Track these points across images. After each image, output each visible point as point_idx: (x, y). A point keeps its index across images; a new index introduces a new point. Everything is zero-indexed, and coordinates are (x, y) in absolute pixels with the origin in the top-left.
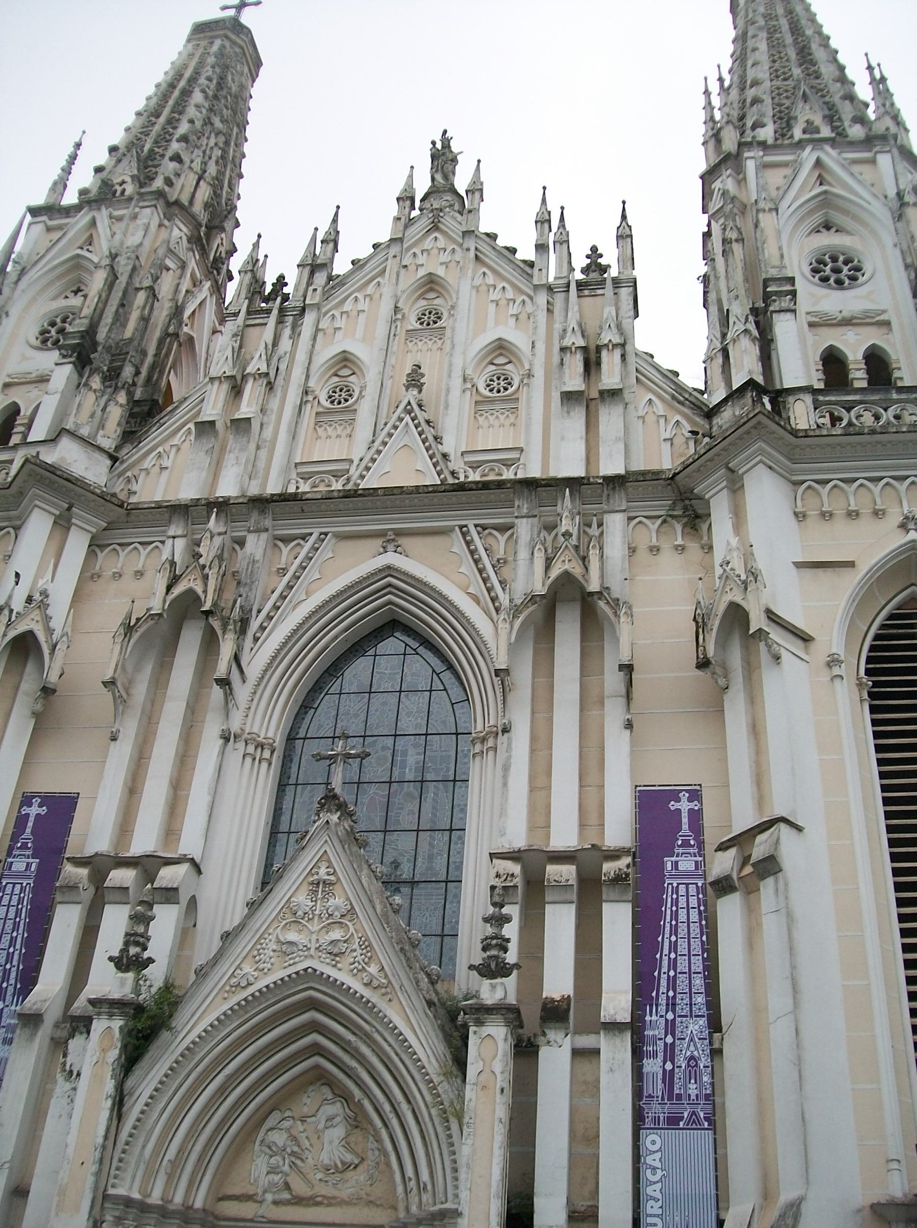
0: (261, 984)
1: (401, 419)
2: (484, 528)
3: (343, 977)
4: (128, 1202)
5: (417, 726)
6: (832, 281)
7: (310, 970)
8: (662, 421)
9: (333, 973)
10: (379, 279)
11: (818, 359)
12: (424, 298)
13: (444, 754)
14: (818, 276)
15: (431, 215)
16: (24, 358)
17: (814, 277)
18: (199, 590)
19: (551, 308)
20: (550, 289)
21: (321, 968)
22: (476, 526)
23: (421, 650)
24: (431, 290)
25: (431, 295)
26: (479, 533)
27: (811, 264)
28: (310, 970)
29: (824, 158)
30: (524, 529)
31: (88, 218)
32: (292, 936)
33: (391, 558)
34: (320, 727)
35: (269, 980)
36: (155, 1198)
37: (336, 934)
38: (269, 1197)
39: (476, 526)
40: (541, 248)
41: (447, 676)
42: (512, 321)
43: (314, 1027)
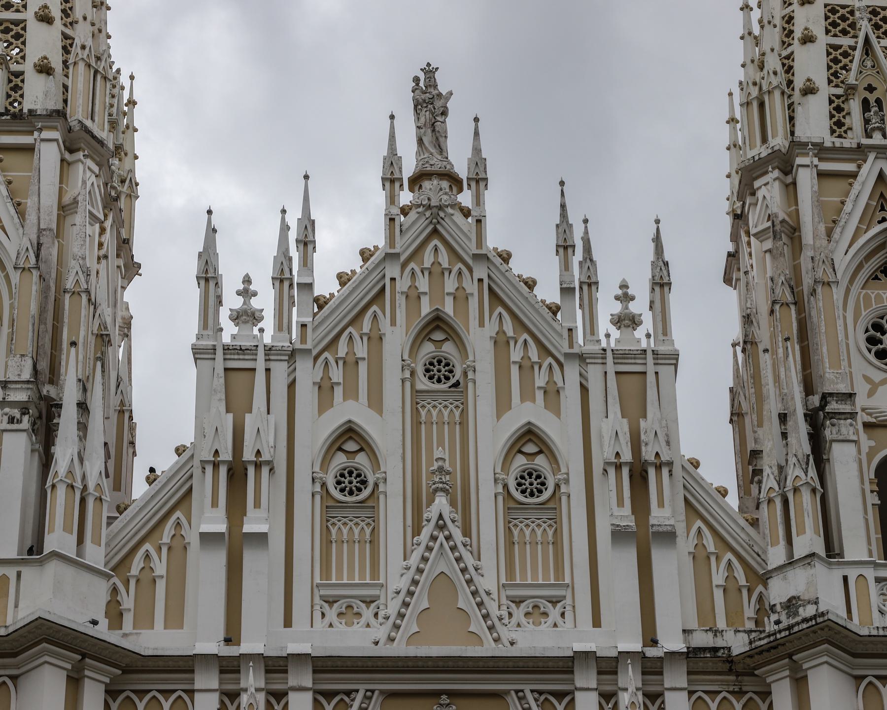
1: (434, 538)
2: (541, 693)
8: (713, 559)
10: (374, 308)
11: (872, 476)
12: (430, 340)
14: (874, 349)
15: (428, 214)
17: (870, 351)
19: (584, 382)
20: (582, 358)
22: (532, 691)
24: (438, 328)
25: (438, 336)
26: (536, 700)
27: (867, 331)
39: (532, 691)
40: (566, 291)
42: (539, 395)
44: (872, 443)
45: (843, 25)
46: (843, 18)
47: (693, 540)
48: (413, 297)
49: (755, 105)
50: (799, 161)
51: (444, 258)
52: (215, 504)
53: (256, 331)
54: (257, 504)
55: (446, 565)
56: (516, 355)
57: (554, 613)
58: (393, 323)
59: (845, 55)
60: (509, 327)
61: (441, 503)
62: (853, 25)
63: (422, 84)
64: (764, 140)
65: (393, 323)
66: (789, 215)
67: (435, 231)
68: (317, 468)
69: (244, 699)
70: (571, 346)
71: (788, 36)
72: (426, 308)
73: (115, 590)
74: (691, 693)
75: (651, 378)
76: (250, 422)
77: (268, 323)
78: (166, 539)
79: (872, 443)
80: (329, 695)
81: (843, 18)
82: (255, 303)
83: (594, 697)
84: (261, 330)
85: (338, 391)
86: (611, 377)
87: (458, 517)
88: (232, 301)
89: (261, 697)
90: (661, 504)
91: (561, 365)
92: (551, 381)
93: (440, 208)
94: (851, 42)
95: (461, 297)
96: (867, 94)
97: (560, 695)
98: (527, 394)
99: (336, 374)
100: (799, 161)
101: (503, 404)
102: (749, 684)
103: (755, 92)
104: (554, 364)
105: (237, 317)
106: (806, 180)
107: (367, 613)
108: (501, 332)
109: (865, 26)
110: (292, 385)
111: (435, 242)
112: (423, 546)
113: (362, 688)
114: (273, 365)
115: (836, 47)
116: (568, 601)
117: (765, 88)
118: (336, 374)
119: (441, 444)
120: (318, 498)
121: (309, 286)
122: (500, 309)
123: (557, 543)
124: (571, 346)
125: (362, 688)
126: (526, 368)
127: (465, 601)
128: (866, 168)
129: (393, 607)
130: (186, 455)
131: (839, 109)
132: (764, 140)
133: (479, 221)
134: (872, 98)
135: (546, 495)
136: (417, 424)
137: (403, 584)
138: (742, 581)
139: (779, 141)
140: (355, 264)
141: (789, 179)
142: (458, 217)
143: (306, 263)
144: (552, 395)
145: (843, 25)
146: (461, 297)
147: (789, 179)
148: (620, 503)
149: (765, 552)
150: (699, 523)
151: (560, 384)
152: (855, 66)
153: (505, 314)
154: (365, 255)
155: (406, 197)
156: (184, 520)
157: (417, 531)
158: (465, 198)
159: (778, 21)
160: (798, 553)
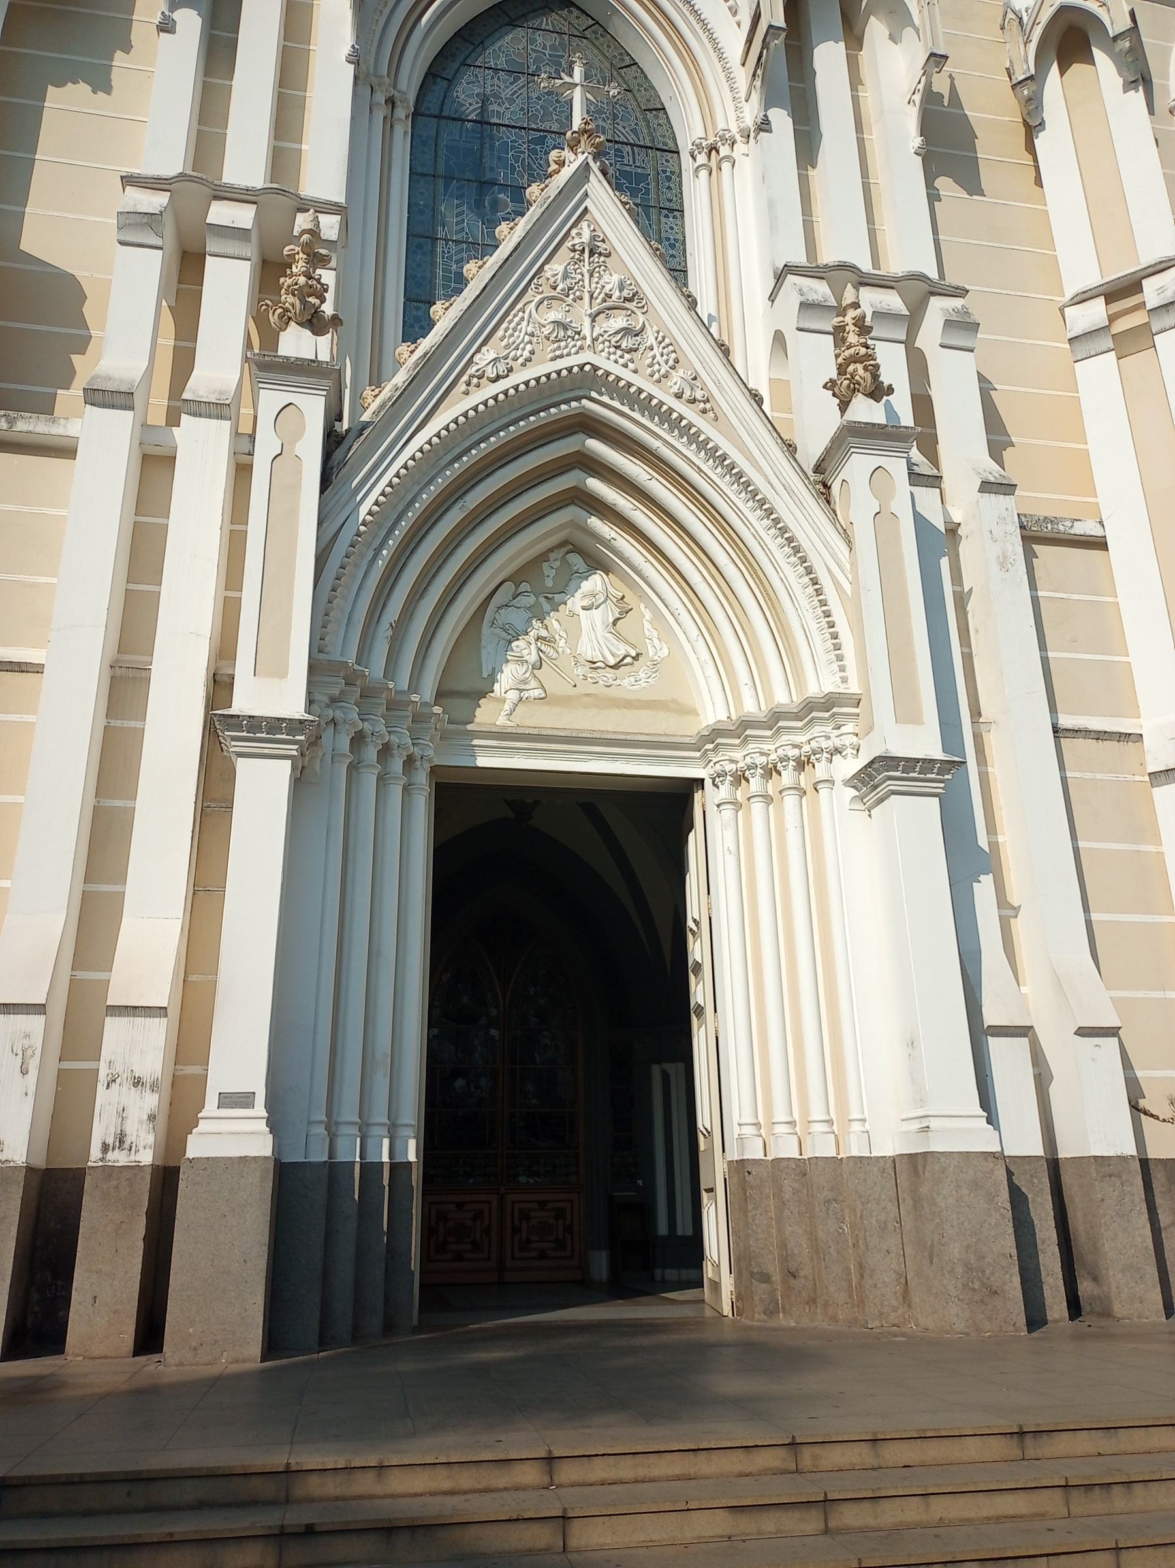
3: (638, 381)
7: (587, 368)
9: (627, 375)
13: (639, 170)
21: (606, 363)
28: (587, 368)
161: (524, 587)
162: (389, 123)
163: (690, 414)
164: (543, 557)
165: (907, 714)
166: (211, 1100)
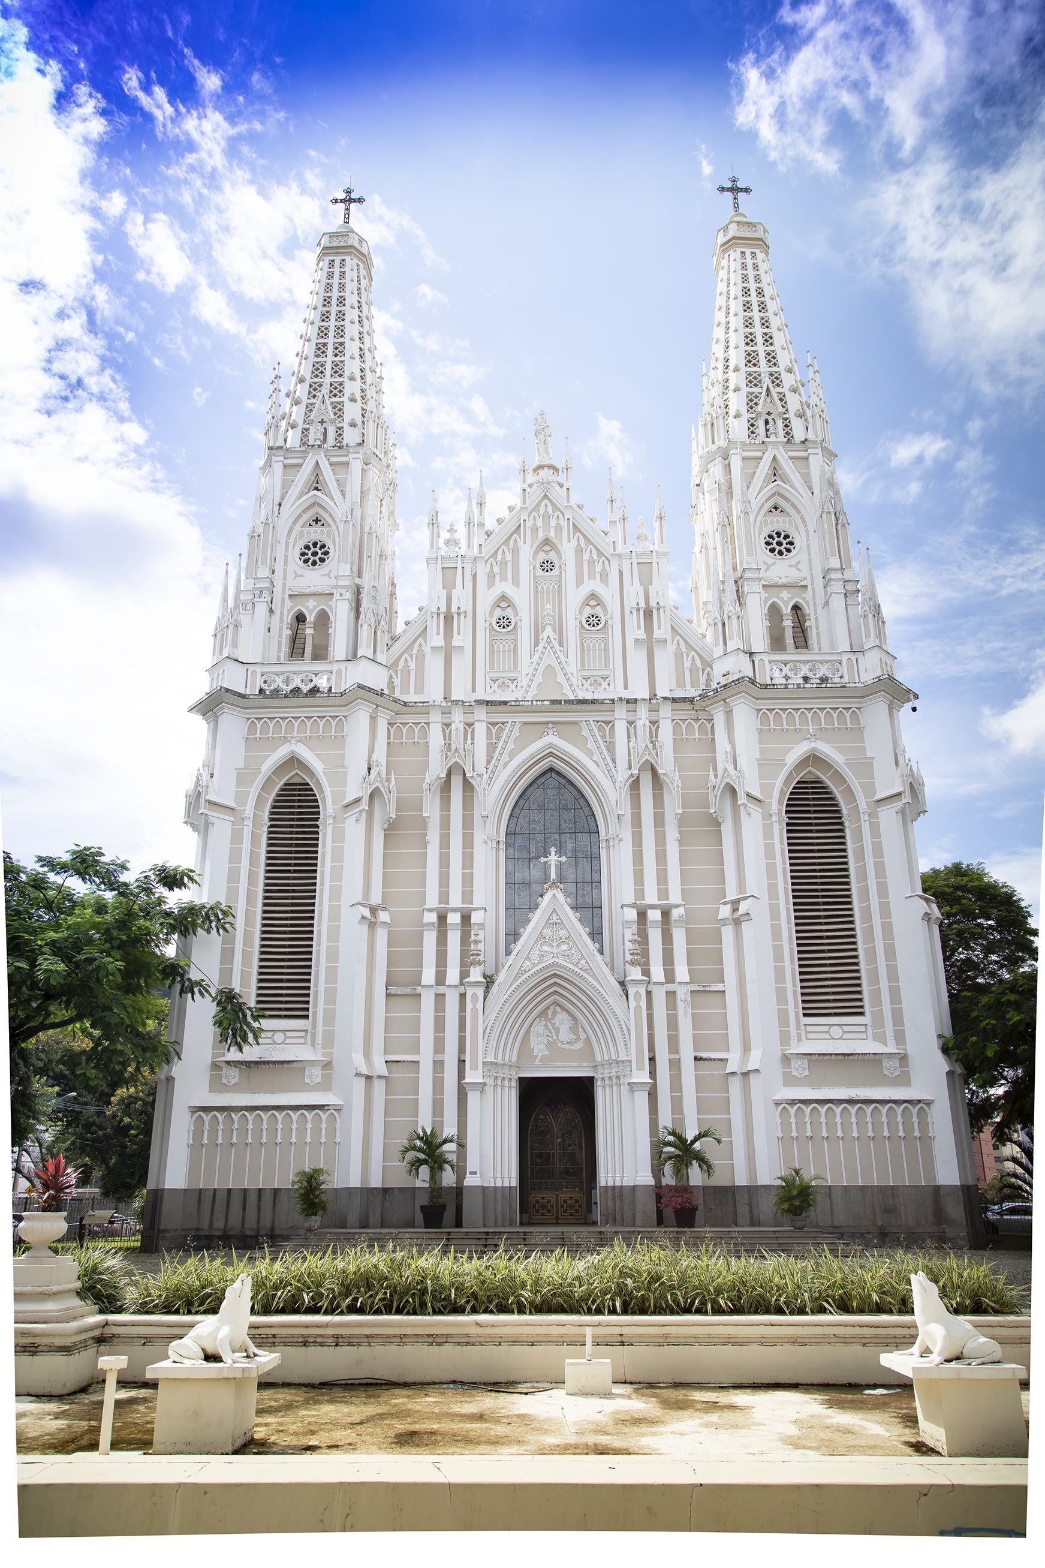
0: (534, 970)
3: (570, 966)
4: (492, 1063)
5: (570, 828)
6: (777, 551)
8: (685, 655)
9: (566, 964)
14: (769, 547)
16: (297, 575)
18: (462, 764)
21: (560, 961)
23: (567, 785)
29: (779, 456)
30: (621, 727)
31: (313, 463)
32: (545, 948)
33: (550, 738)
34: (522, 828)
35: (538, 968)
36: (500, 1060)
37: (564, 947)
38: (540, 1055)
41: (581, 801)
42: (598, 576)
43: (555, 984)
44: (767, 595)
45: (755, 382)
46: (755, 378)
47: (675, 646)
48: (535, 529)
49: (709, 425)
50: (732, 451)
51: (550, 509)
52: (438, 633)
53: (457, 549)
54: (459, 633)
55: (549, 660)
56: (586, 556)
57: (604, 684)
58: (525, 542)
59: (756, 397)
60: (582, 543)
61: (549, 631)
62: (760, 382)
63: (539, 420)
64: (713, 443)
65: (525, 542)
66: (726, 480)
67: (546, 495)
68: (487, 615)
69: (453, 726)
70: (614, 550)
71: (726, 389)
72: (541, 535)
73: (391, 677)
74: (673, 720)
75: (655, 565)
76: (455, 593)
77: (463, 544)
78: (415, 651)
79: (767, 595)
80: (494, 724)
81: (755, 378)
82: (456, 536)
83: (624, 724)
84: (460, 548)
85: (498, 577)
86: (635, 567)
87: (557, 637)
88: (445, 535)
89: (461, 726)
90: (659, 628)
91: (609, 561)
92: (604, 569)
93: (548, 483)
94: (760, 390)
95: (558, 529)
96: (767, 417)
97: (607, 723)
98: (592, 576)
99: (497, 569)
100: (732, 451)
101: (580, 581)
102: (702, 715)
103: (709, 419)
104: (606, 561)
105: (447, 543)
106: (736, 462)
107: (512, 686)
108: (579, 545)
109: (767, 381)
110: (475, 576)
111: (546, 501)
112: (540, 652)
113: (510, 721)
114: (465, 565)
115: (752, 393)
116: (612, 677)
117: (714, 416)
118: (497, 569)
119: (548, 602)
120: (488, 630)
121: (481, 525)
122: (578, 534)
123: (606, 649)
124: (614, 550)
125: (510, 721)
126: (591, 563)
127: (560, 678)
128: (767, 453)
129: (525, 682)
130: (424, 611)
131: (752, 425)
132: (713, 443)
133: (568, 489)
134: (770, 418)
135: (601, 626)
136: (536, 592)
137: (530, 670)
138: (699, 665)
139: (722, 442)
140: (505, 514)
141: (726, 462)
142: (558, 488)
143: (481, 513)
144: (604, 577)
145: (755, 382)
146: (558, 529)
147: (726, 462)
148: (639, 628)
149: (712, 651)
150: (678, 637)
151: (608, 570)
152: (761, 403)
153: (581, 537)
154: (511, 509)
155: (531, 478)
156: (423, 643)
157: (537, 644)
158: (561, 478)
159: (721, 381)
160: (730, 648)
161: (543, 1019)
162: (498, 849)
163: (585, 975)
164: (548, 1008)
165: (640, 1068)
166: (468, 1173)
